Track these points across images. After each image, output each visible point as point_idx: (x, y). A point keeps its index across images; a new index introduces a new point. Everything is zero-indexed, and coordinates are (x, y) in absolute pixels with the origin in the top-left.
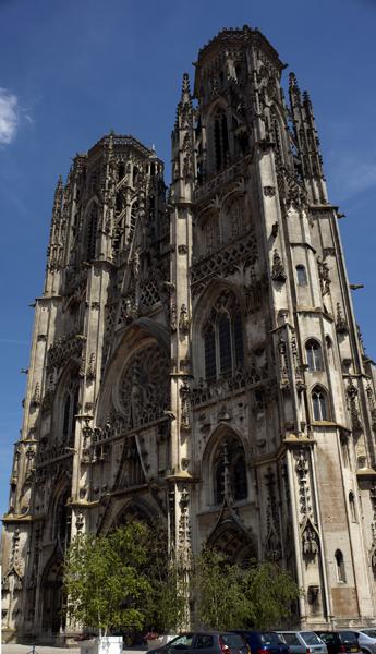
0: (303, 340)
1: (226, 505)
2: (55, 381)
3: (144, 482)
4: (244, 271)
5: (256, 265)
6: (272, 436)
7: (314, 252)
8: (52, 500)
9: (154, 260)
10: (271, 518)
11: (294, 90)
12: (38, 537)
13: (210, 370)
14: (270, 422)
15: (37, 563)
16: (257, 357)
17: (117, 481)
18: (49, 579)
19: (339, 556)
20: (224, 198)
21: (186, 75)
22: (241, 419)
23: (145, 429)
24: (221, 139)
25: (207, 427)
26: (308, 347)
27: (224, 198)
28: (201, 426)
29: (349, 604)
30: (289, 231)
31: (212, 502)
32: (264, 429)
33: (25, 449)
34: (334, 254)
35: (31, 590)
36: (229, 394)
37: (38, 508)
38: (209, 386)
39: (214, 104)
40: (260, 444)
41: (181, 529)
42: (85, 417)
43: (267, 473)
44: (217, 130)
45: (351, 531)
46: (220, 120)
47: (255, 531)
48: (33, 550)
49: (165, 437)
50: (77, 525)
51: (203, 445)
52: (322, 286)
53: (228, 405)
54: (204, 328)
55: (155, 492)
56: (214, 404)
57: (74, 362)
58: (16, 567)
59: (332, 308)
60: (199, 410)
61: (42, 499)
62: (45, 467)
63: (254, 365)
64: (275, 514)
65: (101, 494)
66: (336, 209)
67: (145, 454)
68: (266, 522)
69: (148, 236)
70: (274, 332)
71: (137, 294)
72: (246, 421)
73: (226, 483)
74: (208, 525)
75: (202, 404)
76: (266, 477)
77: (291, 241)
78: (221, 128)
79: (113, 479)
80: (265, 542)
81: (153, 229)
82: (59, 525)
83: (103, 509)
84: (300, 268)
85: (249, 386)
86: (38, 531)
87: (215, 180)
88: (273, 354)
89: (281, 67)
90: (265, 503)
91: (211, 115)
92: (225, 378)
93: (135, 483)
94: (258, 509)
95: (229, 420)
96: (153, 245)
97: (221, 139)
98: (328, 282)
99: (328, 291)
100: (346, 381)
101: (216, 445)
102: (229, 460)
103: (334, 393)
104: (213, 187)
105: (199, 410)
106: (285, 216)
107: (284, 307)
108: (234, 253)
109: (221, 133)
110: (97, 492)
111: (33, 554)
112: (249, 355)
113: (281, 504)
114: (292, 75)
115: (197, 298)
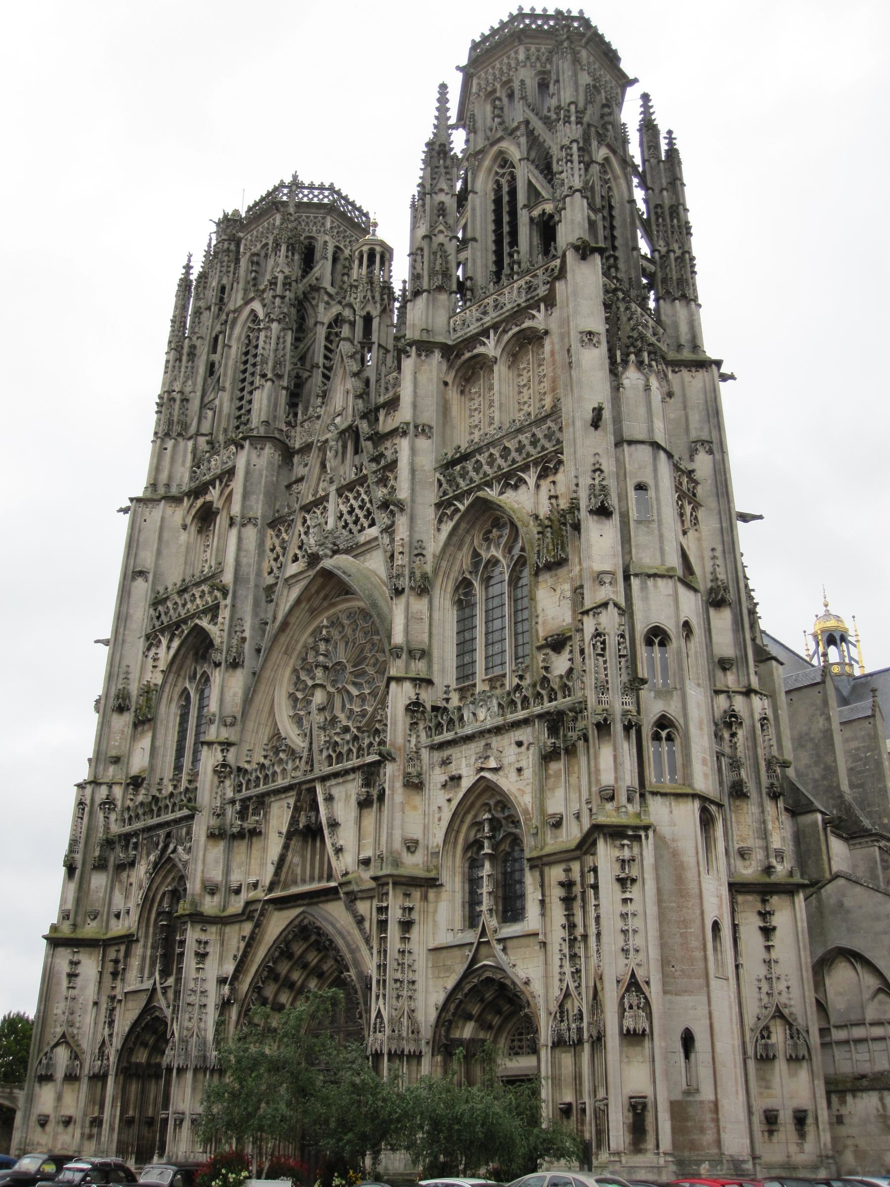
0: (641, 629)
1: (483, 933)
2: (162, 665)
3: (330, 877)
4: (538, 486)
5: (560, 477)
6: (575, 807)
7: (670, 456)
8: (147, 902)
9: (368, 446)
10: (567, 963)
11: (648, 127)
12: (115, 974)
13: (465, 672)
14: (573, 779)
15: (111, 1023)
16: (553, 656)
17: (277, 873)
18: (133, 1059)
19: (688, 1040)
20: (506, 337)
21: (443, 87)
22: (519, 770)
23: (336, 775)
24: (506, 218)
25: (456, 779)
26: (649, 643)
27: (506, 337)
28: (444, 778)
29: (702, 1130)
30: (624, 416)
31: (458, 925)
32: (560, 793)
34: (710, 452)
36: (499, 721)
37: (118, 916)
38: (461, 699)
39: (495, 149)
40: (552, 821)
41: (399, 975)
43: (562, 877)
44: (498, 201)
45: (713, 995)
46: (503, 181)
47: (537, 987)
48: (104, 1000)
49: (375, 793)
50: (197, 954)
51: (447, 815)
52: (682, 515)
53: (496, 742)
54: (457, 589)
57: (202, 629)
59: (702, 558)
60: (441, 746)
61: (127, 897)
62: (136, 834)
63: (546, 669)
64: (574, 957)
65: (244, 896)
66: (718, 363)
67: (334, 825)
68: (557, 970)
69: (360, 396)
70: (586, 612)
71: (331, 506)
72: (528, 773)
73: (486, 888)
74: (449, 969)
75: (448, 736)
76: (561, 884)
77: (627, 435)
78: (506, 198)
79: (270, 870)
80: (554, 1007)
81: (367, 382)
82: (160, 952)
84: (641, 487)
86: (116, 961)
87: (490, 300)
88: (582, 652)
89: (626, 82)
90: (557, 935)
91: (490, 170)
92: (493, 688)
93: (312, 879)
94: (544, 944)
95: (495, 770)
96: (364, 416)
97: (506, 218)
98: (696, 506)
99: (695, 521)
100: (722, 698)
101: (469, 819)
102: (494, 847)
103: (693, 730)
104: (485, 313)
105: (441, 746)
106: (617, 388)
107: (607, 568)
108: (519, 450)
109: (506, 208)
110: (238, 891)
111: (104, 1006)
112: (540, 648)
113: (585, 937)
114: (645, 97)
115: (447, 527)
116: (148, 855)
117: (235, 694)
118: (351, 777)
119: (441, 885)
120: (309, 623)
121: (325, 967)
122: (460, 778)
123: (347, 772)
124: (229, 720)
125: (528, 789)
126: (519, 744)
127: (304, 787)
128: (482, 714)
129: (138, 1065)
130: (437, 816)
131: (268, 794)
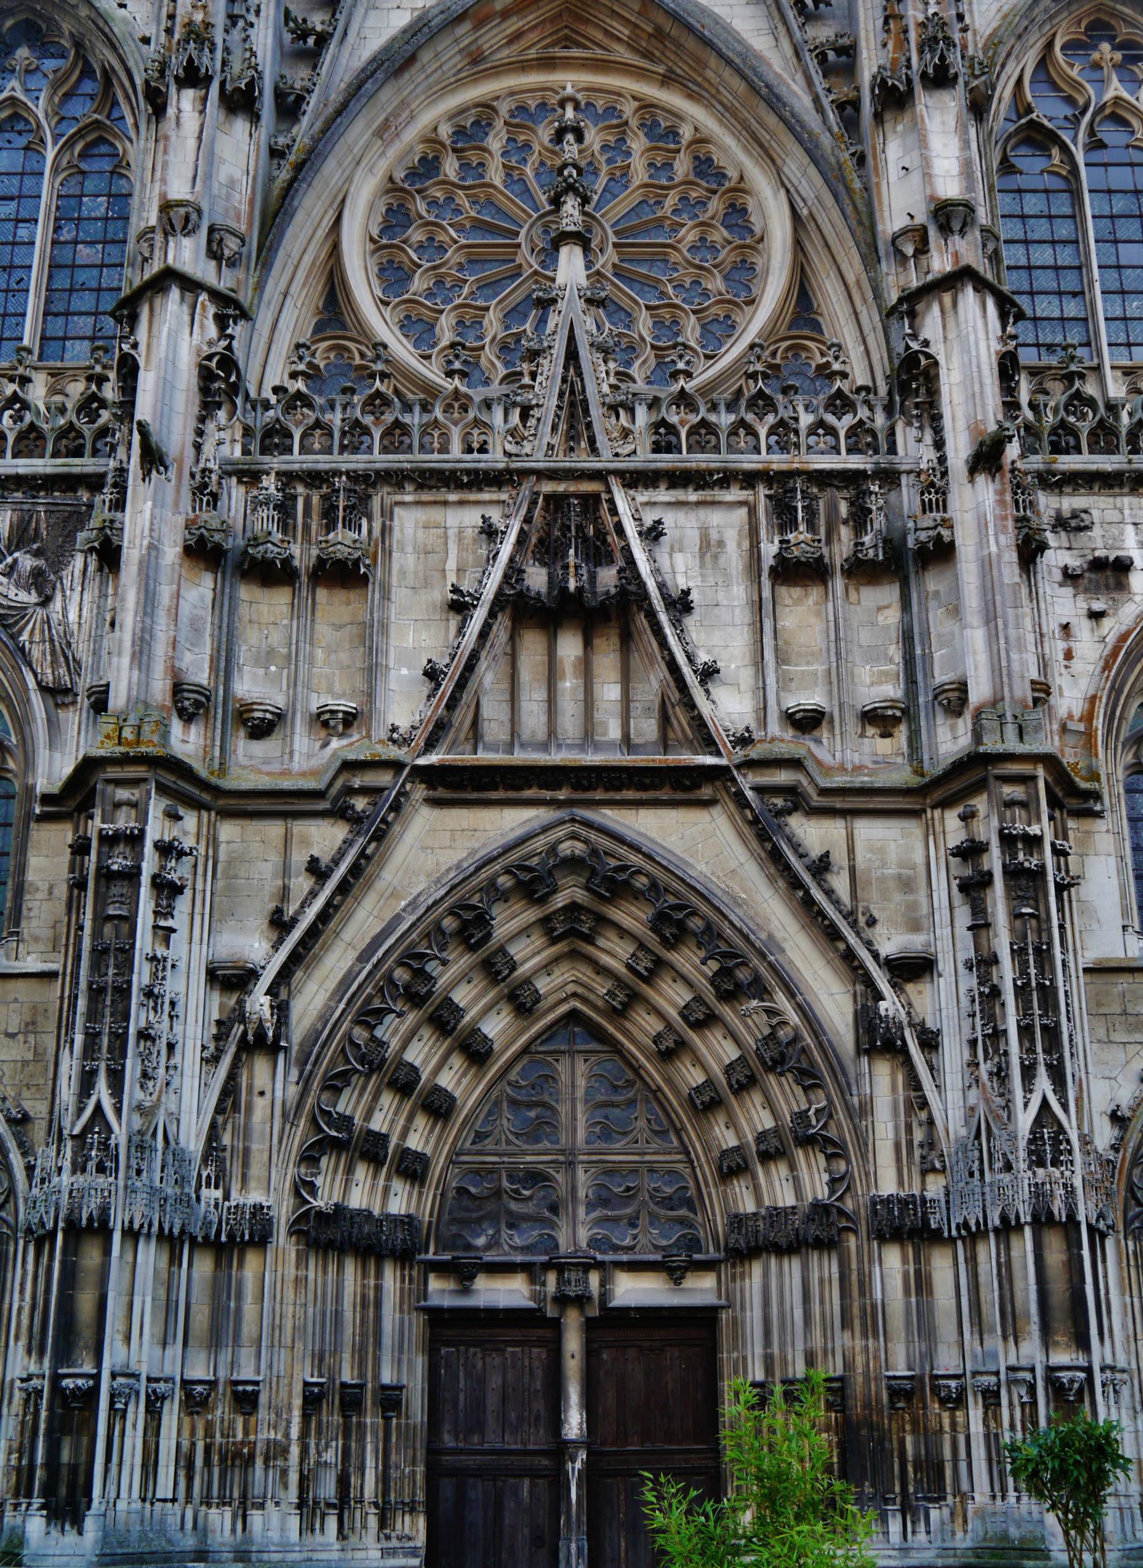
23: (679, 479)
42: (216, 295)
117: (232, 184)
118: (735, 494)
119: (1098, 815)
120: (460, 83)
121: (542, 985)
122: (1123, 567)
123: (727, 478)
124: (232, 245)
127: (548, 487)
130: (1061, 645)
131: (396, 478)
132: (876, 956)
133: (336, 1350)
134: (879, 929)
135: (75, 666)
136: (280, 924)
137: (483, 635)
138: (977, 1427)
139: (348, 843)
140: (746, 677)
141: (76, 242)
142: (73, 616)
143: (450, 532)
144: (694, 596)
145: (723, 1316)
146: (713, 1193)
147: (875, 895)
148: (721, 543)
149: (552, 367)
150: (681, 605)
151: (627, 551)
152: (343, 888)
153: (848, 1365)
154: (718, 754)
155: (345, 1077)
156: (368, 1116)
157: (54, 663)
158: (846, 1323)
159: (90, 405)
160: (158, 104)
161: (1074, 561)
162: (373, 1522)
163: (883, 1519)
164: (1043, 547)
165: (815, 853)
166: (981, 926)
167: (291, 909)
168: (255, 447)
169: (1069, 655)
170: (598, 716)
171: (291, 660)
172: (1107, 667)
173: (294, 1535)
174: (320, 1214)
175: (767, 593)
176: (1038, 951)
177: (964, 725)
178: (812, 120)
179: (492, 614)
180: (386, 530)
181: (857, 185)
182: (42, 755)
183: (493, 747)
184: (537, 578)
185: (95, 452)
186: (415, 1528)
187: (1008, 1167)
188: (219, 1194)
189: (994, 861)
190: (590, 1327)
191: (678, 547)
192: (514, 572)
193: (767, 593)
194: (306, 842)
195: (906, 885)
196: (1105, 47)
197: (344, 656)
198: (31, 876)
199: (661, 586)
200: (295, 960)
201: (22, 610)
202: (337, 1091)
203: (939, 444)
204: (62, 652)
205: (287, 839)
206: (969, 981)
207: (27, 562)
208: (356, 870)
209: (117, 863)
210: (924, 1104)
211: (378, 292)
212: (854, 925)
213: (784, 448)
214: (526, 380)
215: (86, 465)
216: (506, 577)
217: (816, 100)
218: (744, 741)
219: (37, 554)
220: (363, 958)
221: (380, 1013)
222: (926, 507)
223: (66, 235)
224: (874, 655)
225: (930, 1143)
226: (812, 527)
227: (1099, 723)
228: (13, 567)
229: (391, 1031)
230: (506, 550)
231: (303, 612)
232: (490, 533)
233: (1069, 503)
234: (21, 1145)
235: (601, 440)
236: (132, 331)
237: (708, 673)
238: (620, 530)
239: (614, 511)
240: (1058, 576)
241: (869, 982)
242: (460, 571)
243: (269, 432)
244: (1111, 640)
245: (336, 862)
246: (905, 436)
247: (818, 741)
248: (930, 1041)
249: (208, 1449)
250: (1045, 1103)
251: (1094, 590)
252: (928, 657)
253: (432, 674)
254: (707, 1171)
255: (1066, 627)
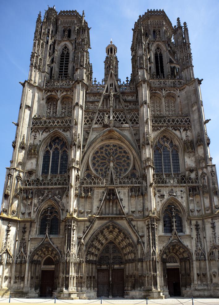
25: (162, 196)
33: (15, 174)
35: (21, 264)
55: (130, 222)
56: (168, 187)
58: (8, 249)
83: (88, 224)
85: (189, 185)
116: (38, 196)
122: (164, 195)
125: (185, 202)
126: (182, 191)
128: (172, 182)
129: (35, 260)
132: (139, 235)
133: (89, 273)
134: (139, 233)
135: (64, 207)
136: (84, 233)
137: (103, 203)
138: (146, 279)
139: (90, 225)
140: (128, 207)
141: (63, 161)
142: (64, 202)
143: (100, 193)
144: (123, 199)
145: (124, 269)
146: (123, 258)
147: (139, 229)
148: (126, 193)
149: (110, 175)
150: (121, 200)
151: (117, 194)
152: (90, 229)
153: (135, 274)
154: (125, 215)
155: (90, 247)
156: (92, 251)
157: (62, 207)
158: (135, 270)
159: (65, 180)
160: (71, 147)
161: (159, 195)
162: (93, 288)
163: (138, 288)
164: (156, 194)
165: (134, 225)
166: (149, 232)
167: (85, 231)
168: (81, 184)
169: (158, 205)
170: (114, 211)
171: (84, 206)
172: (162, 206)
173: (86, 290)
174: (88, 261)
175: (130, 199)
176: (154, 235)
177: (148, 212)
178: (135, 147)
179: (104, 201)
180: (94, 193)
181: (140, 155)
182: (61, 216)
183: (104, 215)
184: (108, 197)
185: (66, 185)
186: (96, 289)
187: (150, 256)
188: (79, 259)
189: (150, 226)
190: (112, 270)
191: (121, 194)
192: (106, 197)
193: (130, 199)
194: (86, 224)
195: (142, 228)
196: (165, 138)
197: (90, 206)
198: (61, 228)
199: (120, 198)
200: (85, 236)
201: (59, 201)
202: (89, 249)
203: (147, 183)
204: (63, 205)
205: (84, 224)
206: (147, 238)
207: (59, 196)
208: (91, 227)
209: (69, 228)
210: (143, 249)
211: (92, 159)
212: (137, 232)
213: (132, 184)
214: (107, 176)
215: (65, 186)
216: (105, 197)
217: (136, 145)
218: (127, 214)
219: (60, 196)
220: (92, 236)
221: (93, 241)
222: (145, 190)
223: (62, 160)
224: (140, 205)
225: (143, 253)
226: (134, 192)
227: (161, 212)
228: (58, 197)
229: (94, 243)
230: (105, 195)
231: (86, 201)
232: (103, 193)
233: (159, 189)
234: (61, 254)
235: (114, 183)
236: (69, 172)
237: (124, 207)
238: (116, 192)
239: (115, 190)
240: (158, 196)
241: (138, 237)
242: (101, 197)
243: (82, 183)
244: (162, 203)
245: (89, 226)
246: (144, 182)
247: (134, 214)
248: (144, 243)
249: (78, 282)
250: (154, 250)
251: (161, 198)
252: (145, 205)
253: (98, 207)
254: (123, 256)
255: (158, 202)
